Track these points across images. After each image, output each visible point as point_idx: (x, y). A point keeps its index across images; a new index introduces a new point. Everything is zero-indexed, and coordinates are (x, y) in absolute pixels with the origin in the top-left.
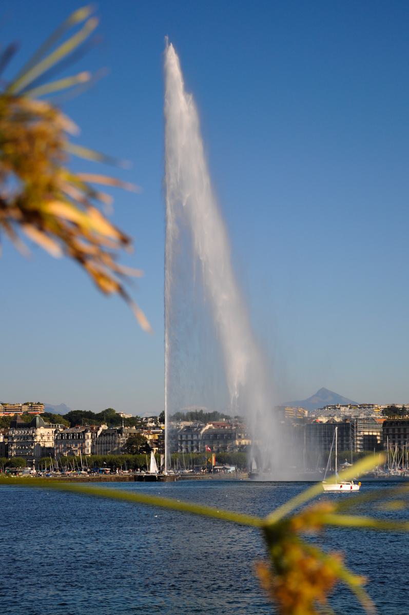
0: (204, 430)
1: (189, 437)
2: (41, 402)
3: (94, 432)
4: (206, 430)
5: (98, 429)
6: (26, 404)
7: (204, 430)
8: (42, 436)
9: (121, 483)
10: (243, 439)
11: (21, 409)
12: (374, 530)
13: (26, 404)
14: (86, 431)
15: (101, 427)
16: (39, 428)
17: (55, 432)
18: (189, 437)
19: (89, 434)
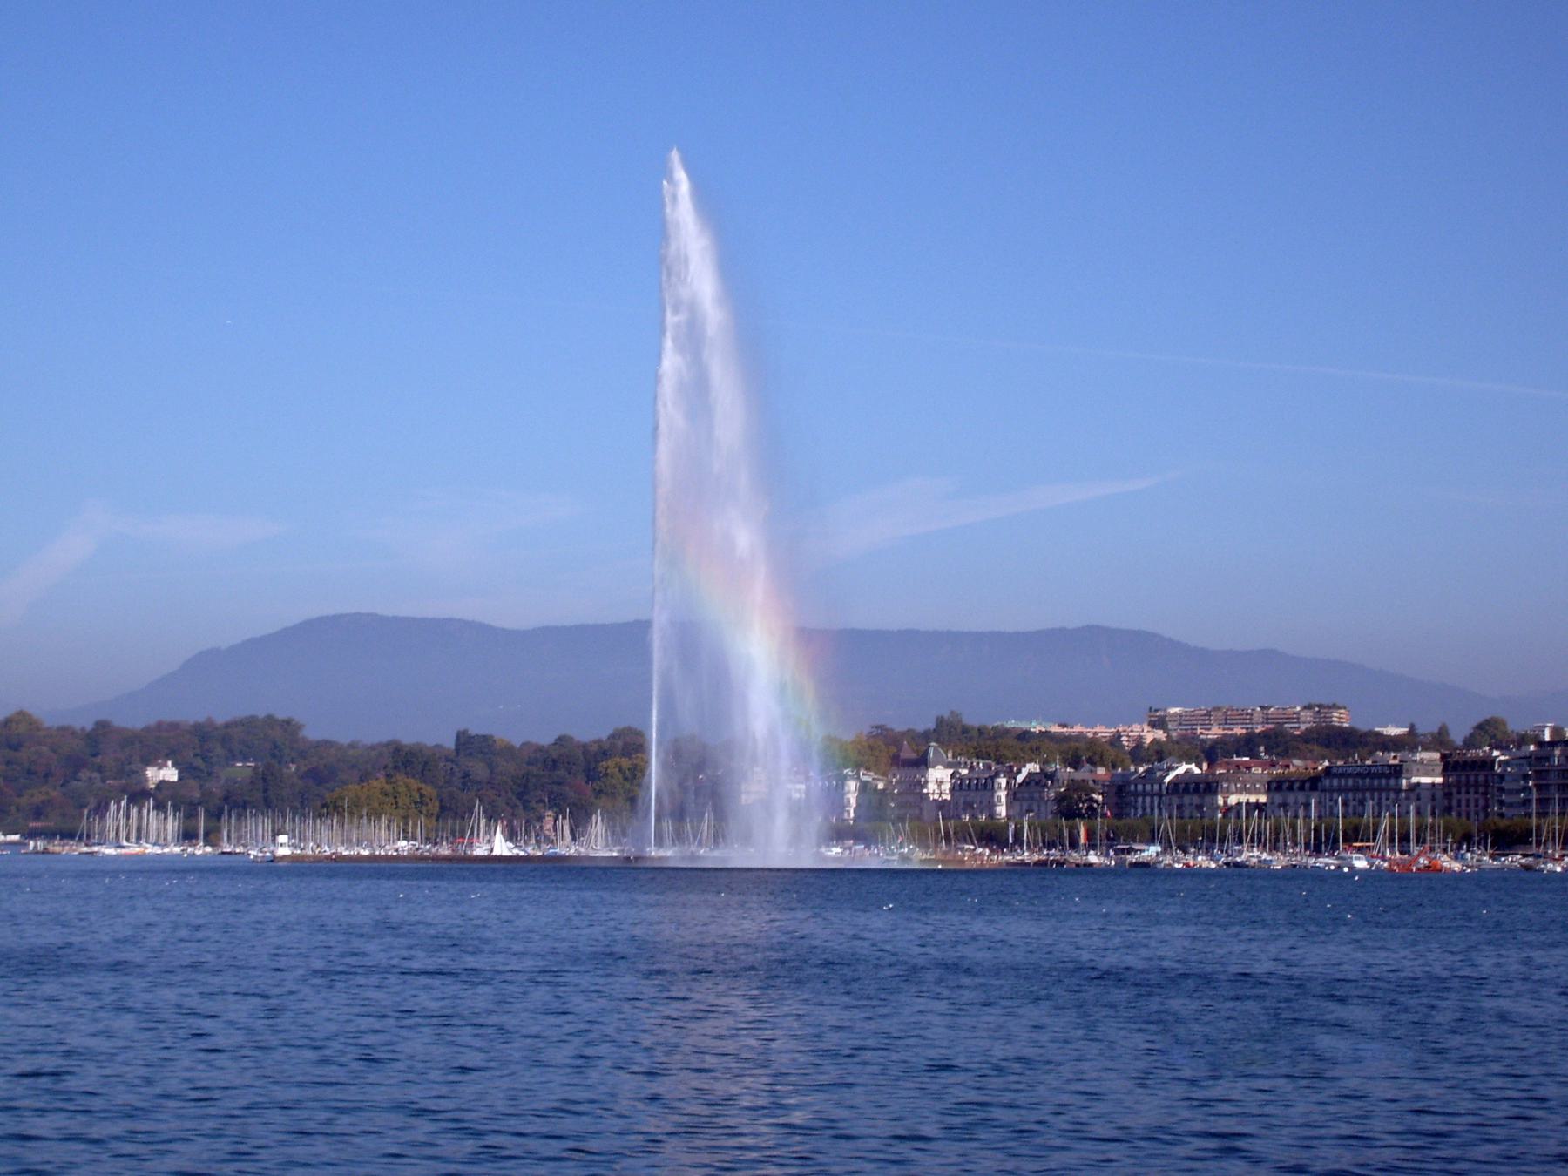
0: (1172, 775)
1: (1148, 787)
2: (1339, 703)
3: (1011, 775)
4: (1177, 775)
5: (1019, 772)
6: (1308, 707)
7: (1172, 775)
8: (940, 783)
9: (405, 882)
10: (1232, 794)
11: (1298, 718)
12: (637, 971)
13: (1308, 707)
14: (997, 775)
15: (1025, 766)
16: (934, 767)
17: (952, 776)
18: (1148, 787)
19: (1003, 781)
